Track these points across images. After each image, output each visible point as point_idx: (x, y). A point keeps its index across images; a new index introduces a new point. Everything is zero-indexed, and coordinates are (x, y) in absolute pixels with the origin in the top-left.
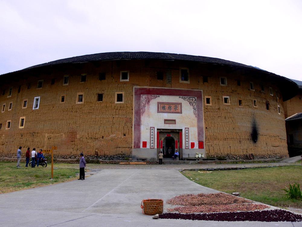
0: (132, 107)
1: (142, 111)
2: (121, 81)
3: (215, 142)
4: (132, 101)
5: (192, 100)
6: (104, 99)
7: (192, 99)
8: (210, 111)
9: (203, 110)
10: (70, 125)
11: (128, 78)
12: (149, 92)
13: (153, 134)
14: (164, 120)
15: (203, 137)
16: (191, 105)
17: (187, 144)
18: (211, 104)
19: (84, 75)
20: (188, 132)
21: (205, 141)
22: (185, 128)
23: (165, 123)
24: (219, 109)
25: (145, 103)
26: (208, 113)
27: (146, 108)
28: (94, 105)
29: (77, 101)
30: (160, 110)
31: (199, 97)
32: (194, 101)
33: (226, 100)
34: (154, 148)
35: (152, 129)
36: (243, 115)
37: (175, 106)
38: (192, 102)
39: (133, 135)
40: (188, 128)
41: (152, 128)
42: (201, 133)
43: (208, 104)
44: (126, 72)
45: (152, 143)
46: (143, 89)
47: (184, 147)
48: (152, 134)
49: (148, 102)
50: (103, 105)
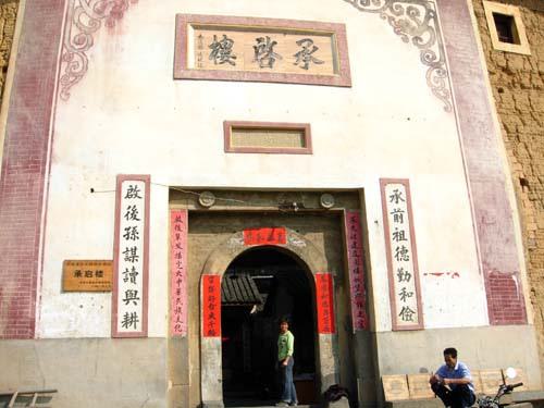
5: (413, 14)
7: (409, 9)
8: (526, 81)
9: (486, 73)
13: (140, 227)
14: (225, 123)
15: (509, 240)
16: (405, 40)
17: (404, 295)
18: (523, 48)
20: (402, 206)
22: (384, 183)
23: (227, 149)
25: (93, 22)
26: (521, 96)
27: (97, 53)
30: (192, 62)
32: (422, 18)
34: (143, 336)
35: (133, 193)
37: (300, 43)
38: (414, 24)
40: (406, 183)
41: (129, 186)
42: (493, 211)
43: (508, 47)
47: (382, 322)
48: (132, 223)
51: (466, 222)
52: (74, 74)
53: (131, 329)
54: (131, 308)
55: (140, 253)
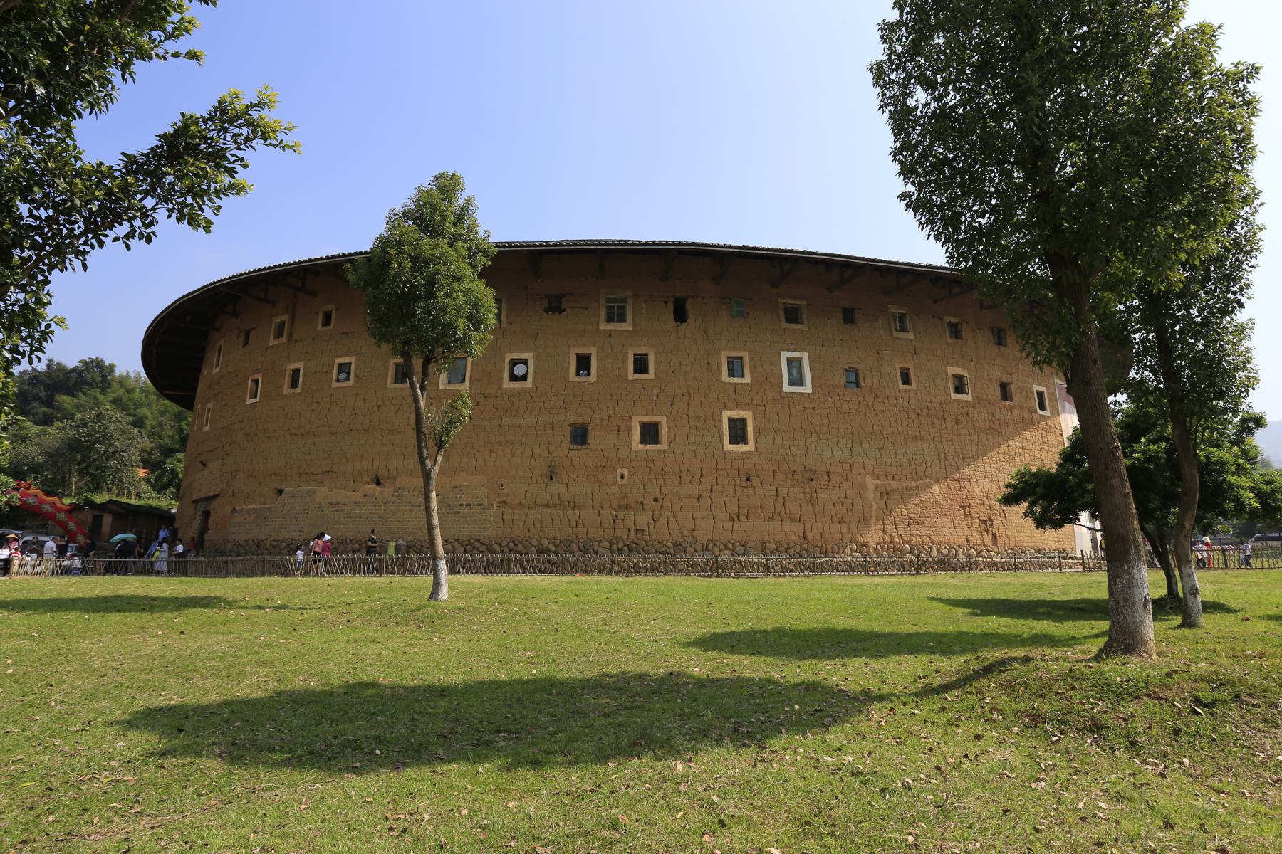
10: (950, 458)
19: (953, 320)
29: (952, 390)
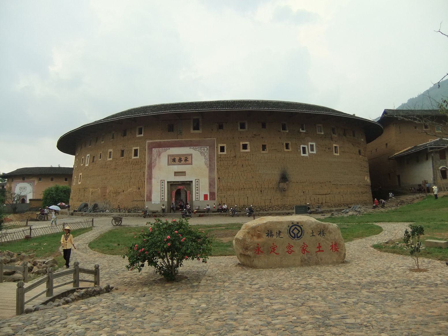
0: (145, 162)
1: (153, 164)
2: (137, 136)
3: (229, 193)
4: (145, 155)
6: (125, 155)
8: (224, 160)
11: (143, 134)
12: (160, 145)
15: (214, 188)
16: (202, 155)
18: (225, 153)
20: (198, 183)
21: (217, 193)
22: (196, 180)
23: (174, 176)
24: (235, 156)
27: (157, 161)
28: (118, 161)
30: (170, 163)
31: (212, 147)
33: (245, 147)
34: (164, 201)
35: (163, 182)
36: (266, 161)
39: (146, 188)
40: (199, 180)
41: (162, 181)
43: (222, 153)
44: (141, 127)
45: (163, 196)
46: (154, 143)
47: (194, 200)
49: (159, 155)
50: (124, 161)
51: (208, 185)
52: (155, 165)
53: (163, 200)
54: (163, 197)
55: (164, 190)
